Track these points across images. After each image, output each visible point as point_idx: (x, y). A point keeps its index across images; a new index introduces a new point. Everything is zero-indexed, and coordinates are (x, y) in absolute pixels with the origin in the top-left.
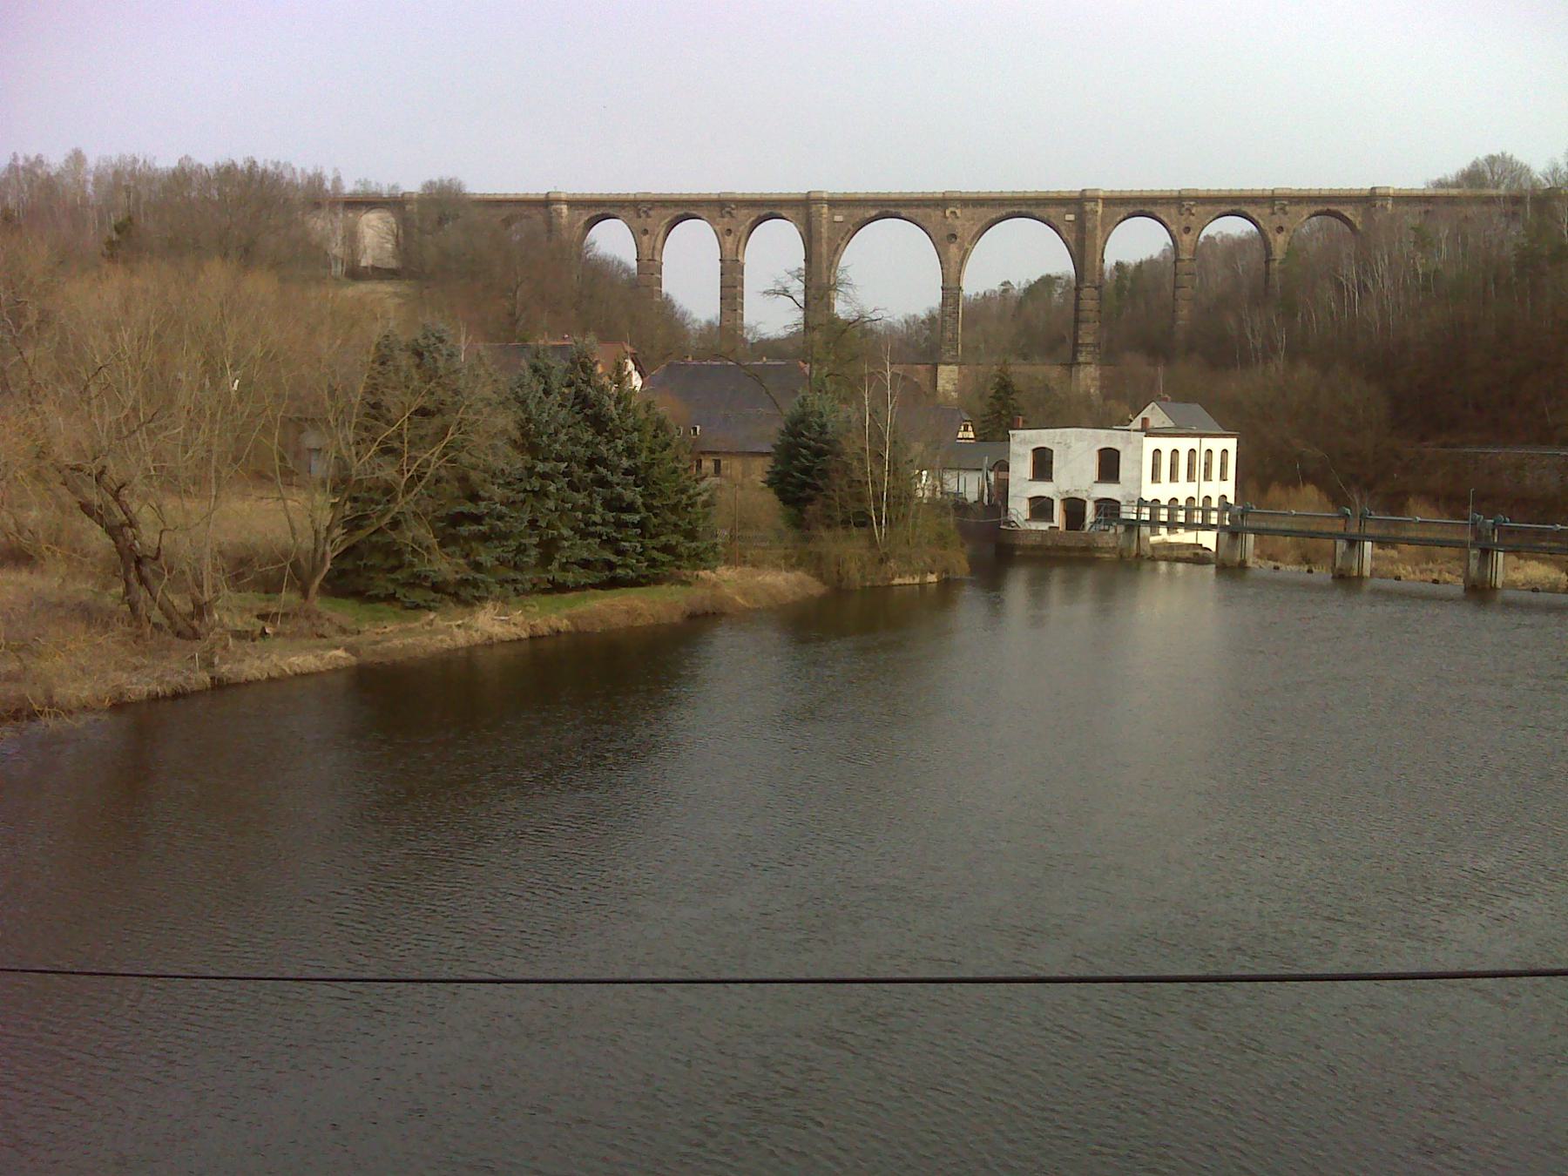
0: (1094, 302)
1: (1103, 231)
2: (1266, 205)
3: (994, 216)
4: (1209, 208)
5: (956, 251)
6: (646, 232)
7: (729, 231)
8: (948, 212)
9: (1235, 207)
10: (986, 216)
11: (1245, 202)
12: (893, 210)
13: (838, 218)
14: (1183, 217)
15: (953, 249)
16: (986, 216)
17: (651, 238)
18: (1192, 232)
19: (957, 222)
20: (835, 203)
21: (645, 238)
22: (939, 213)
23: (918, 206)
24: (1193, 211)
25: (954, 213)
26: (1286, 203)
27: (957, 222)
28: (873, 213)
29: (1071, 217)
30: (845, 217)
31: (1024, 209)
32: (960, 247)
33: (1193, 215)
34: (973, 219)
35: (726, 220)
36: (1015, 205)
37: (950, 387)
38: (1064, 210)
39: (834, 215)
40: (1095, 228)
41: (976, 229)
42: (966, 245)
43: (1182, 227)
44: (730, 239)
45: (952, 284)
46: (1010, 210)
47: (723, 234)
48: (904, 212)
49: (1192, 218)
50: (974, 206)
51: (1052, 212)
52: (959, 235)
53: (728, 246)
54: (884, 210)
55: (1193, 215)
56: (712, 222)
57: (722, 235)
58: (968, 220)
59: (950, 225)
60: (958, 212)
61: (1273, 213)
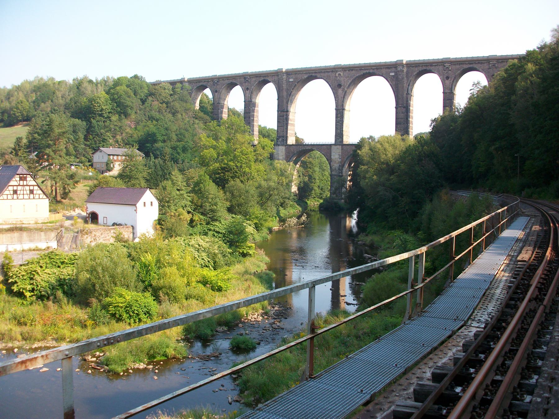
0: (402, 114)
1: (408, 80)
2: (486, 64)
3: (358, 75)
4: (458, 66)
5: (341, 92)
6: (216, 91)
7: (248, 89)
8: (337, 75)
9: (471, 66)
10: (354, 75)
11: (475, 63)
12: (314, 75)
13: (291, 80)
14: (445, 72)
15: (340, 91)
16: (354, 75)
17: (218, 94)
18: (450, 79)
19: (342, 79)
20: (289, 73)
21: (216, 94)
22: (333, 74)
23: (324, 72)
24: (450, 69)
25: (340, 74)
26: (495, 62)
27: (342, 79)
28: (306, 76)
29: (393, 74)
30: (294, 79)
31: (371, 71)
32: (343, 90)
33: (450, 70)
34: (348, 77)
35: (246, 84)
36: (367, 69)
37: (337, 156)
38: (390, 70)
39: (289, 79)
40: (403, 78)
41: (350, 81)
42: (346, 89)
43: (445, 77)
44: (248, 92)
45: (340, 108)
46: (365, 72)
47: (245, 90)
48: (318, 75)
49: (449, 72)
50: (349, 71)
51: (384, 71)
52: (343, 84)
53: (247, 95)
54: (310, 75)
55: (450, 70)
56: (241, 86)
57: (245, 91)
58: (346, 78)
59: (338, 80)
60: (342, 74)
61: (489, 68)
